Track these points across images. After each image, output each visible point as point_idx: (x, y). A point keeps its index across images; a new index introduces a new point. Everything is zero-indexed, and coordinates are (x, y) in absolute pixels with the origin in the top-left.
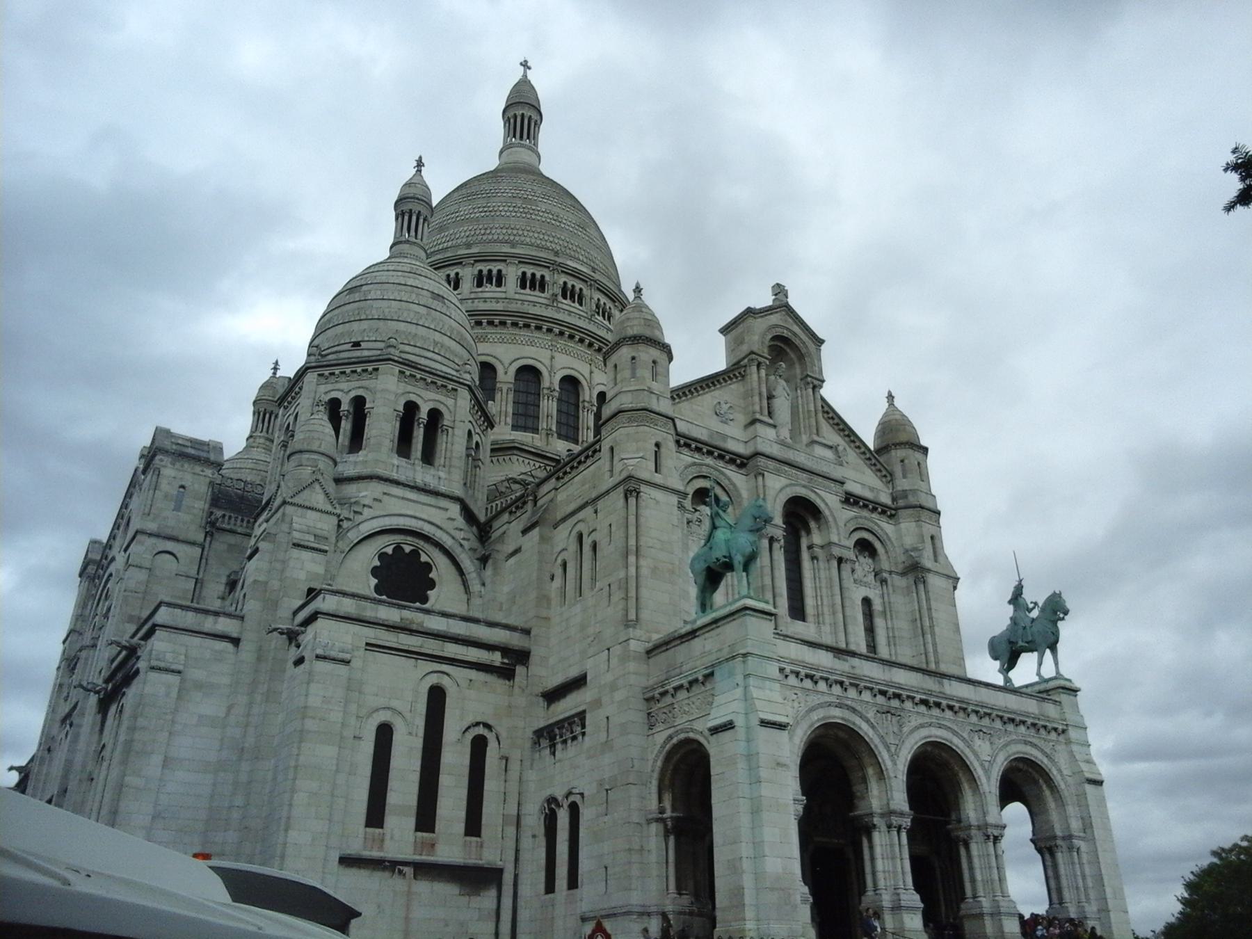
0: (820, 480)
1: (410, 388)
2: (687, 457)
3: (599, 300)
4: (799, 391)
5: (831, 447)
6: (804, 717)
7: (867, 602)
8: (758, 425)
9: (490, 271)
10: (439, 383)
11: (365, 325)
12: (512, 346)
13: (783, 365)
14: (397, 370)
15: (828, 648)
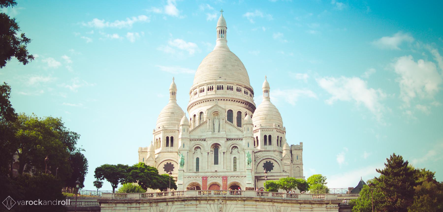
0: (220, 138)
1: (166, 134)
2: (193, 142)
3: (228, 86)
4: (220, 121)
5: (225, 131)
6: (188, 183)
7: (235, 158)
8: (207, 132)
9: (202, 88)
10: (172, 131)
11: (160, 123)
12: (206, 106)
13: (216, 117)
14: (164, 131)
15: (193, 172)
